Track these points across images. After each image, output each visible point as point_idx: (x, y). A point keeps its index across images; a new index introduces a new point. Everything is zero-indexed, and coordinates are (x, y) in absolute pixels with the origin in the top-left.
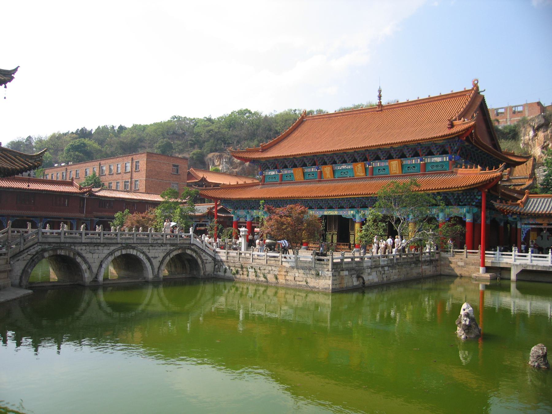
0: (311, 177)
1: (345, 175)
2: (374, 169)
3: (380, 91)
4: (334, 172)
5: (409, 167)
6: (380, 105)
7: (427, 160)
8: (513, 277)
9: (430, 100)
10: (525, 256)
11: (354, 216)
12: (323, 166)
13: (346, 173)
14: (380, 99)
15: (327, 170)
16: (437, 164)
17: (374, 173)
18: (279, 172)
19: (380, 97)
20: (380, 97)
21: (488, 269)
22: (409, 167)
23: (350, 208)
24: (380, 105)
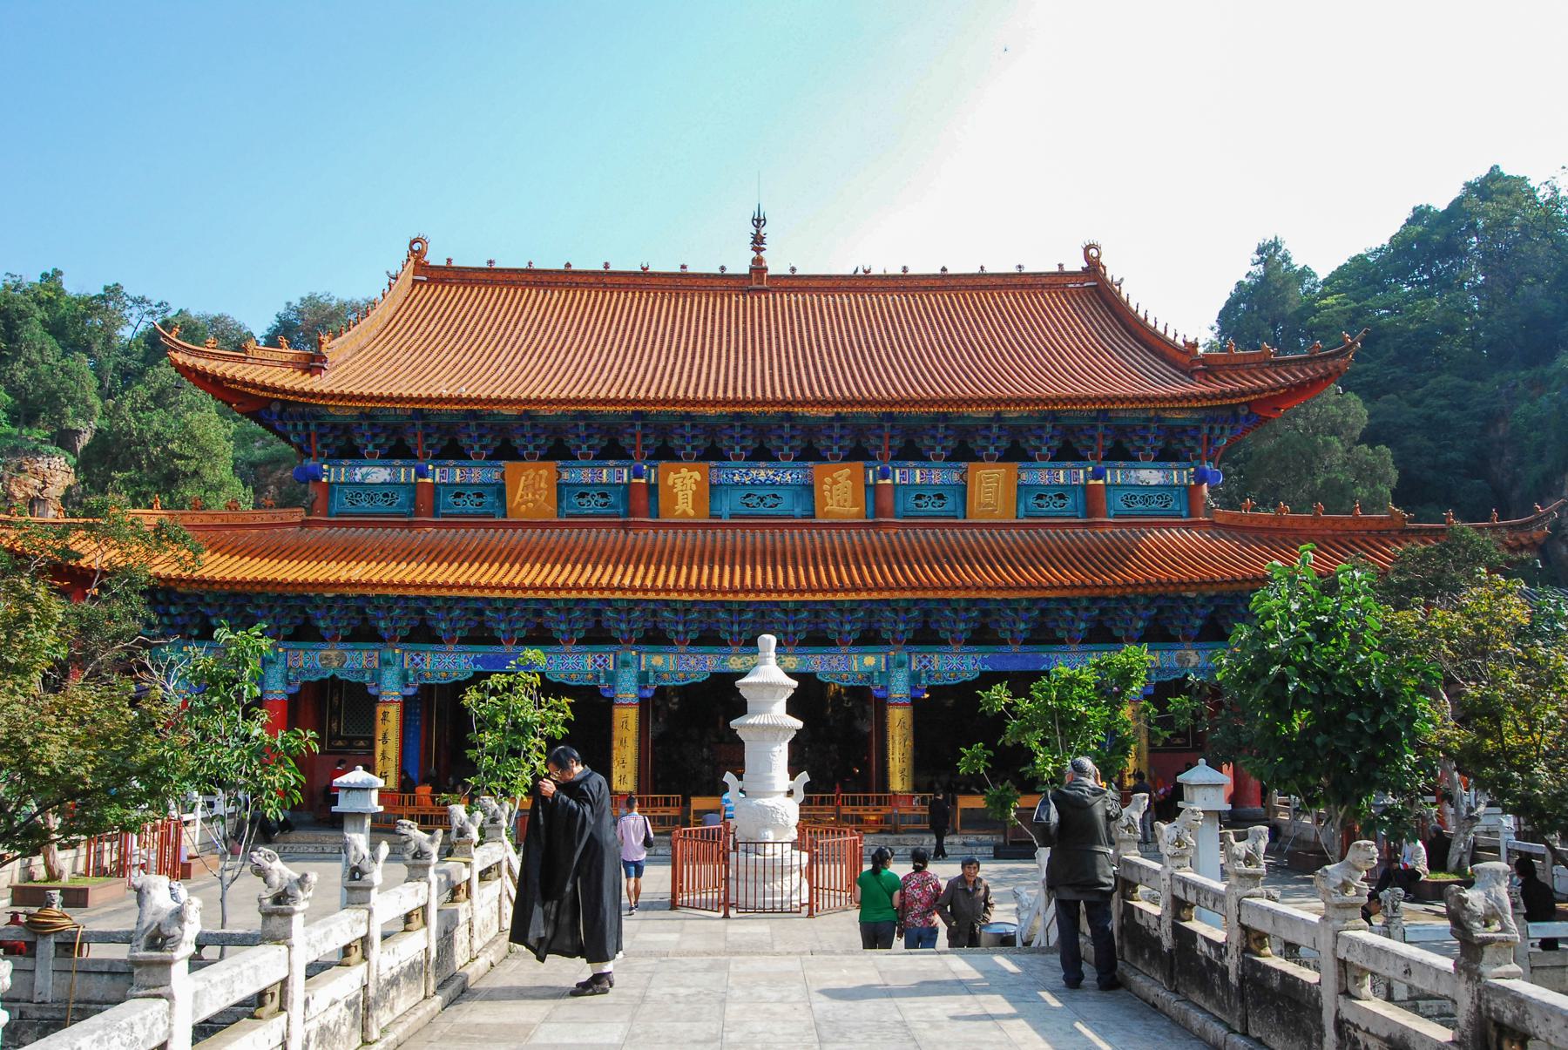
0: (592, 505)
1: (762, 509)
2: (900, 495)
3: (759, 222)
4: (715, 489)
6: (758, 267)
7: (1114, 476)
9: (944, 283)
12: (663, 464)
13: (769, 501)
14: (758, 250)
15: (683, 484)
17: (900, 508)
18: (421, 473)
19: (758, 242)
20: (758, 242)
23: (856, 643)
24: (758, 267)
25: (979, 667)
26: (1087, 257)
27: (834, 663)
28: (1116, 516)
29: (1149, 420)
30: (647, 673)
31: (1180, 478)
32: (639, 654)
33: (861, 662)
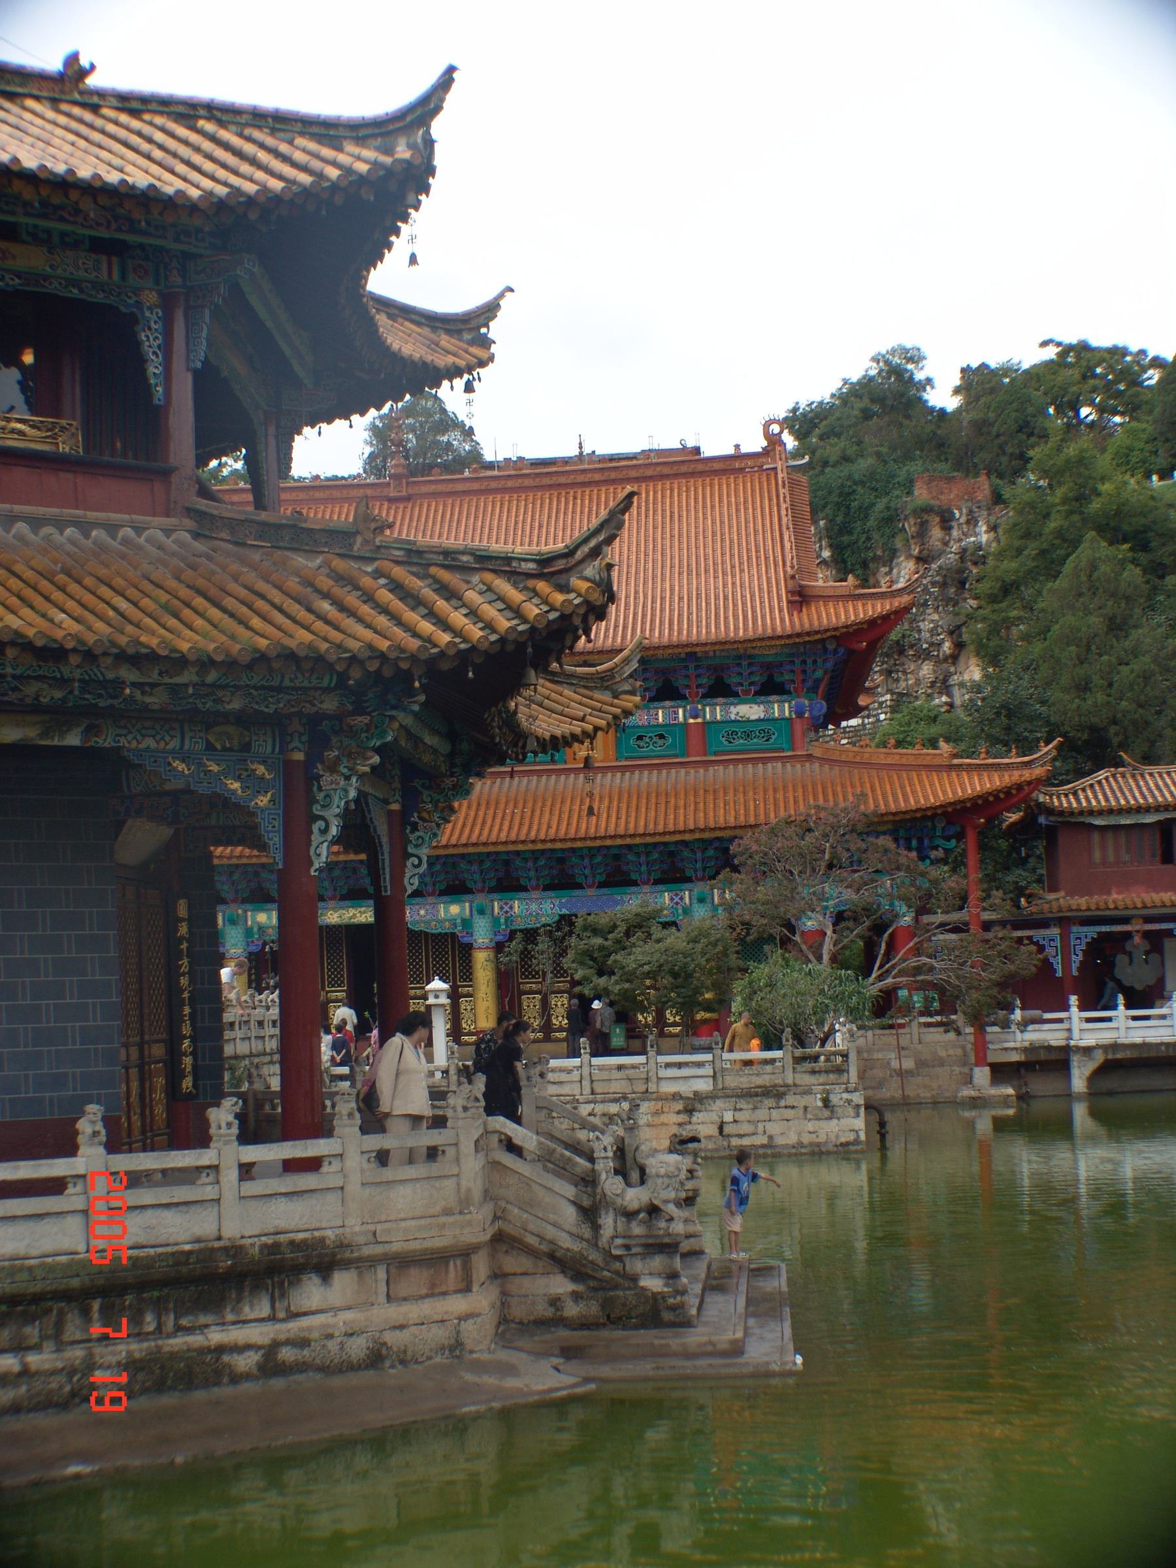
5: (640, 738)
8: (1078, 1082)
10: (1109, 1019)
11: (467, 923)
16: (747, 729)
21: (1000, 1072)
22: (640, 738)
23: (442, 893)
25: (557, 911)
26: (767, 435)
27: (422, 912)
28: (716, 754)
29: (740, 657)
30: (252, 928)
31: (782, 710)
32: (245, 912)
33: (447, 911)
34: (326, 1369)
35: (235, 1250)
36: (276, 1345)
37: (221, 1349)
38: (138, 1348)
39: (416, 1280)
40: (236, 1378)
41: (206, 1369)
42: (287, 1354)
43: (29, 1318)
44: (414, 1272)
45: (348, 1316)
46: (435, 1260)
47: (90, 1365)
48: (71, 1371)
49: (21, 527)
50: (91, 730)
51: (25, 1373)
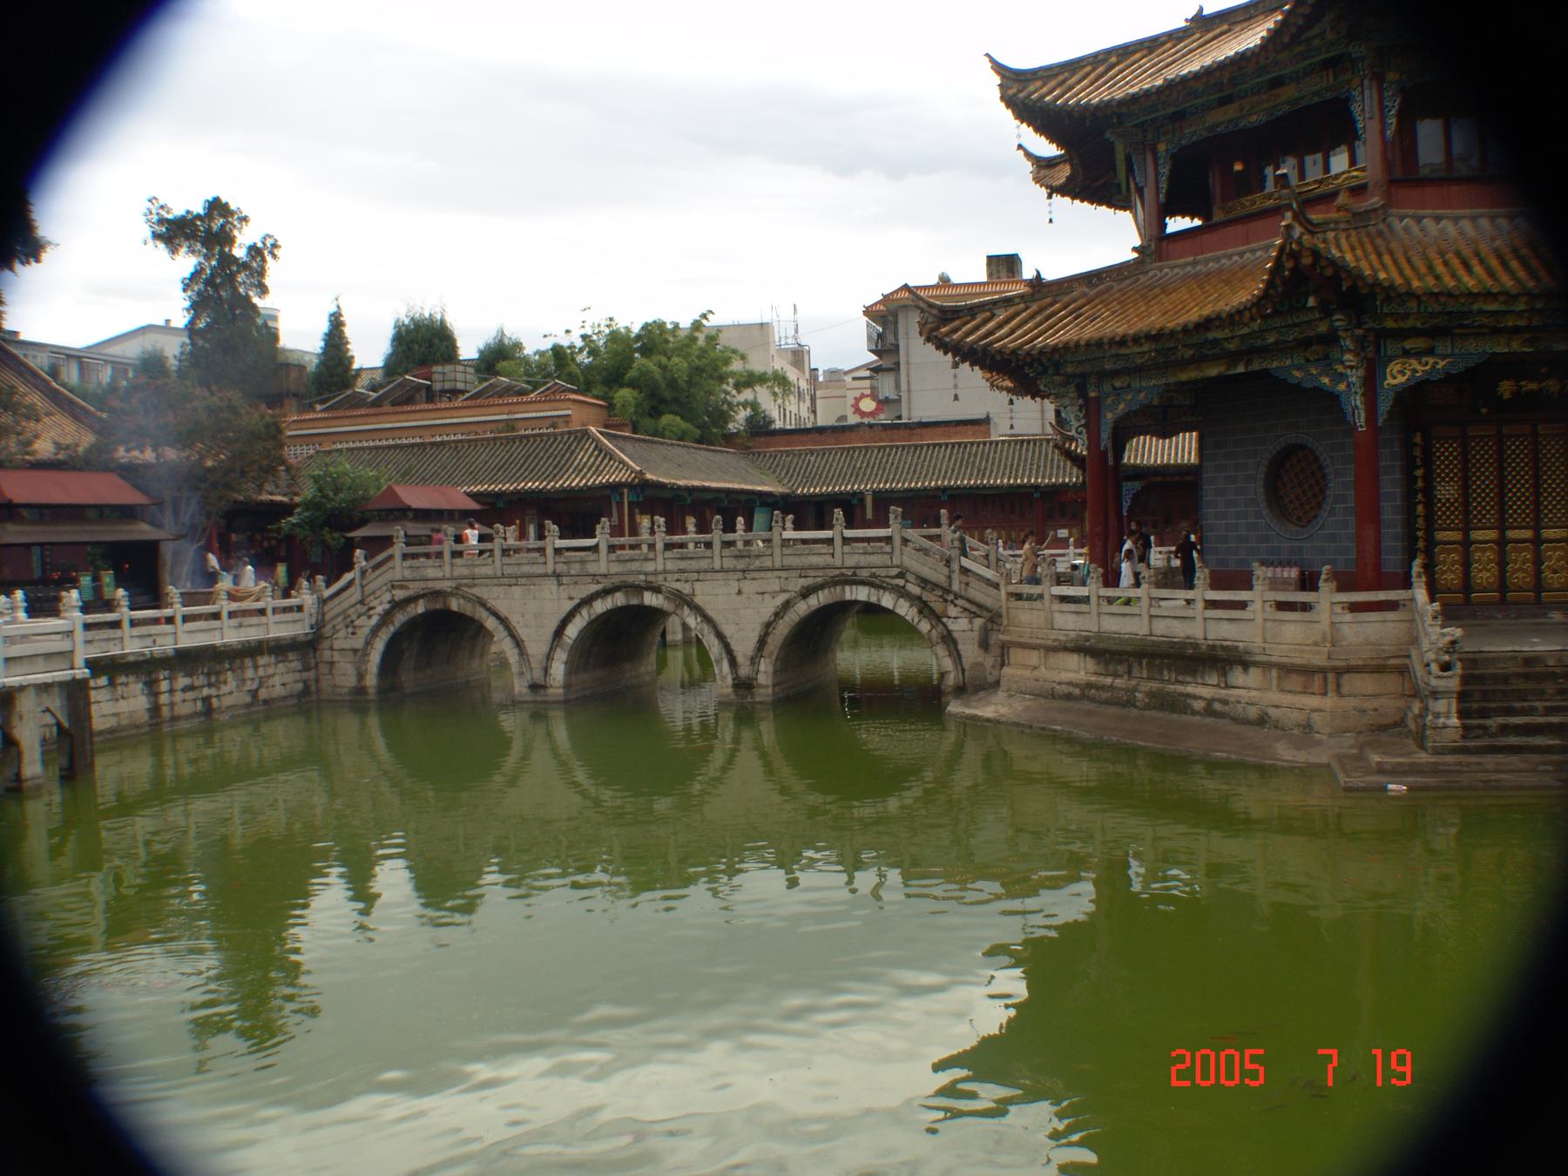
34: (1235, 720)
35: (1196, 646)
36: (1214, 700)
37: (1188, 695)
38: (1155, 685)
39: (1295, 682)
40: (1194, 713)
41: (1178, 704)
42: (1217, 706)
43: (1120, 662)
44: (1294, 676)
45: (1254, 693)
46: (1307, 671)
47: (1135, 689)
48: (1127, 690)
49: (1248, 255)
50: (1249, 362)
51: (1111, 687)
